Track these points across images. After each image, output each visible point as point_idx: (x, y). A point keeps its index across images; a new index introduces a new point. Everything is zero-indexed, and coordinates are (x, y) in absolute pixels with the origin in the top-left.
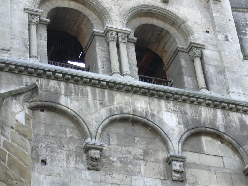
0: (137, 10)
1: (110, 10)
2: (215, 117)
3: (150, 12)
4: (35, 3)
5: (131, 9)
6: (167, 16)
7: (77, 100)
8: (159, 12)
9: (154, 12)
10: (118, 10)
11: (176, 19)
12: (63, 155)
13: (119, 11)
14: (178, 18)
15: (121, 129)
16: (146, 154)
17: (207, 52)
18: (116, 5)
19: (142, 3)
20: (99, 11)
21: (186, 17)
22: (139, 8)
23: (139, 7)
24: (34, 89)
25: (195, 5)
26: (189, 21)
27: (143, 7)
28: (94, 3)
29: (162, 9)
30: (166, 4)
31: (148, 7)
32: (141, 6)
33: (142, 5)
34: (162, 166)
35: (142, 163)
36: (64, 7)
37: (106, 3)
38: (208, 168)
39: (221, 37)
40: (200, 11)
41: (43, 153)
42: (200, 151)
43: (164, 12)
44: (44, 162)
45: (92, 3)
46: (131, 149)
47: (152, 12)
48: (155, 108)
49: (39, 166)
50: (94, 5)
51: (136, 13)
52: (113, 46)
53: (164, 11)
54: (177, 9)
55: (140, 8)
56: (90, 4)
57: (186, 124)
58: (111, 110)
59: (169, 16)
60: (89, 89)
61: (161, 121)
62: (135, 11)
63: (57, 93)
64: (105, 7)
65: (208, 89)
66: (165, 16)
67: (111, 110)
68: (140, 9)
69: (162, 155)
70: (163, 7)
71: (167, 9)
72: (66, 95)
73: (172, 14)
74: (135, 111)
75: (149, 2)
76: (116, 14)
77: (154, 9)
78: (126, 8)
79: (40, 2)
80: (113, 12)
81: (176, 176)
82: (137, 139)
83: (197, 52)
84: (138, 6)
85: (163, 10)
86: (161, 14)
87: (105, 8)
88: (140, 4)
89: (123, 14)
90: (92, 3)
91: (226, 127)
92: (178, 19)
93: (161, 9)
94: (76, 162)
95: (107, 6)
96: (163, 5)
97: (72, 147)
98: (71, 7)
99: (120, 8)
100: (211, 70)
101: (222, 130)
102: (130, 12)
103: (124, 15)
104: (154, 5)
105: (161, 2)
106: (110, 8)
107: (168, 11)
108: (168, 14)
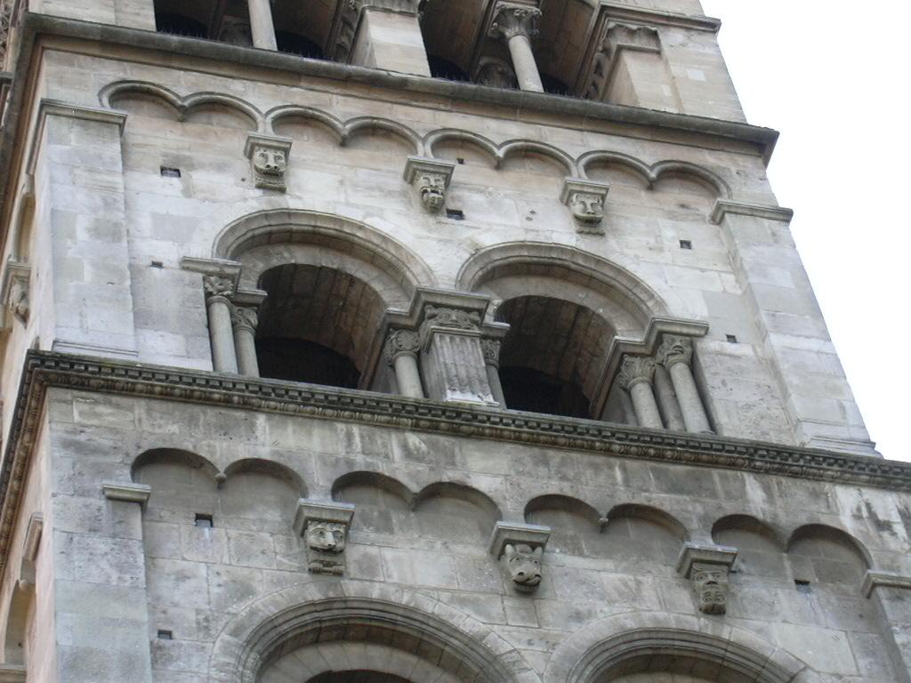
0: (613, 651)
1: (517, 664)
3: (662, 652)
4: (241, 669)
5: (591, 650)
6: (725, 664)
8: (696, 651)
9: (676, 652)
10: (545, 661)
11: (759, 668)
13: (547, 661)
14: (767, 665)
18: (536, 641)
19: (631, 624)
20: (476, 670)
21: (798, 659)
22: (621, 644)
23: (621, 641)
25: (824, 612)
26: (810, 672)
27: (637, 636)
28: (456, 642)
29: (705, 636)
30: (716, 618)
31: (654, 635)
32: (627, 636)
33: (633, 632)
36: (349, 669)
37: (500, 640)
40: (846, 632)
43: (712, 649)
45: (446, 645)
47: (670, 652)
50: (456, 649)
51: (612, 663)
53: (715, 643)
54: (759, 631)
55: (625, 643)
56: (442, 646)
59: (736, 663)
62: (607, 654)
64: (498, 653)
66: (720, 662)
68: (624, 647)
70: (709, 632)
71: (725, 636)
73: (742, 653)
75: (656, 619)
76: (541, 676)
77: (677, 643)
78: (573, 647)
79: (260, 663)
80: (528, 666)
84: (618, 637)
85: (708, 641)
86: (705, 657)
87: (495, 658)
88: (622, 627)
89: (565, 671)
90: (446, 645)
92: (768, 670)
93: (701, 640)
95: (502, 651)
96: (707, 622)
98: (371, 667)
99: (550, 651)
102: (590, 663)
103: (569, 674)
104: (674, 626)
105: (700, 613)
106: (514, 654)
107: (729, 643)
108: (728, 655)
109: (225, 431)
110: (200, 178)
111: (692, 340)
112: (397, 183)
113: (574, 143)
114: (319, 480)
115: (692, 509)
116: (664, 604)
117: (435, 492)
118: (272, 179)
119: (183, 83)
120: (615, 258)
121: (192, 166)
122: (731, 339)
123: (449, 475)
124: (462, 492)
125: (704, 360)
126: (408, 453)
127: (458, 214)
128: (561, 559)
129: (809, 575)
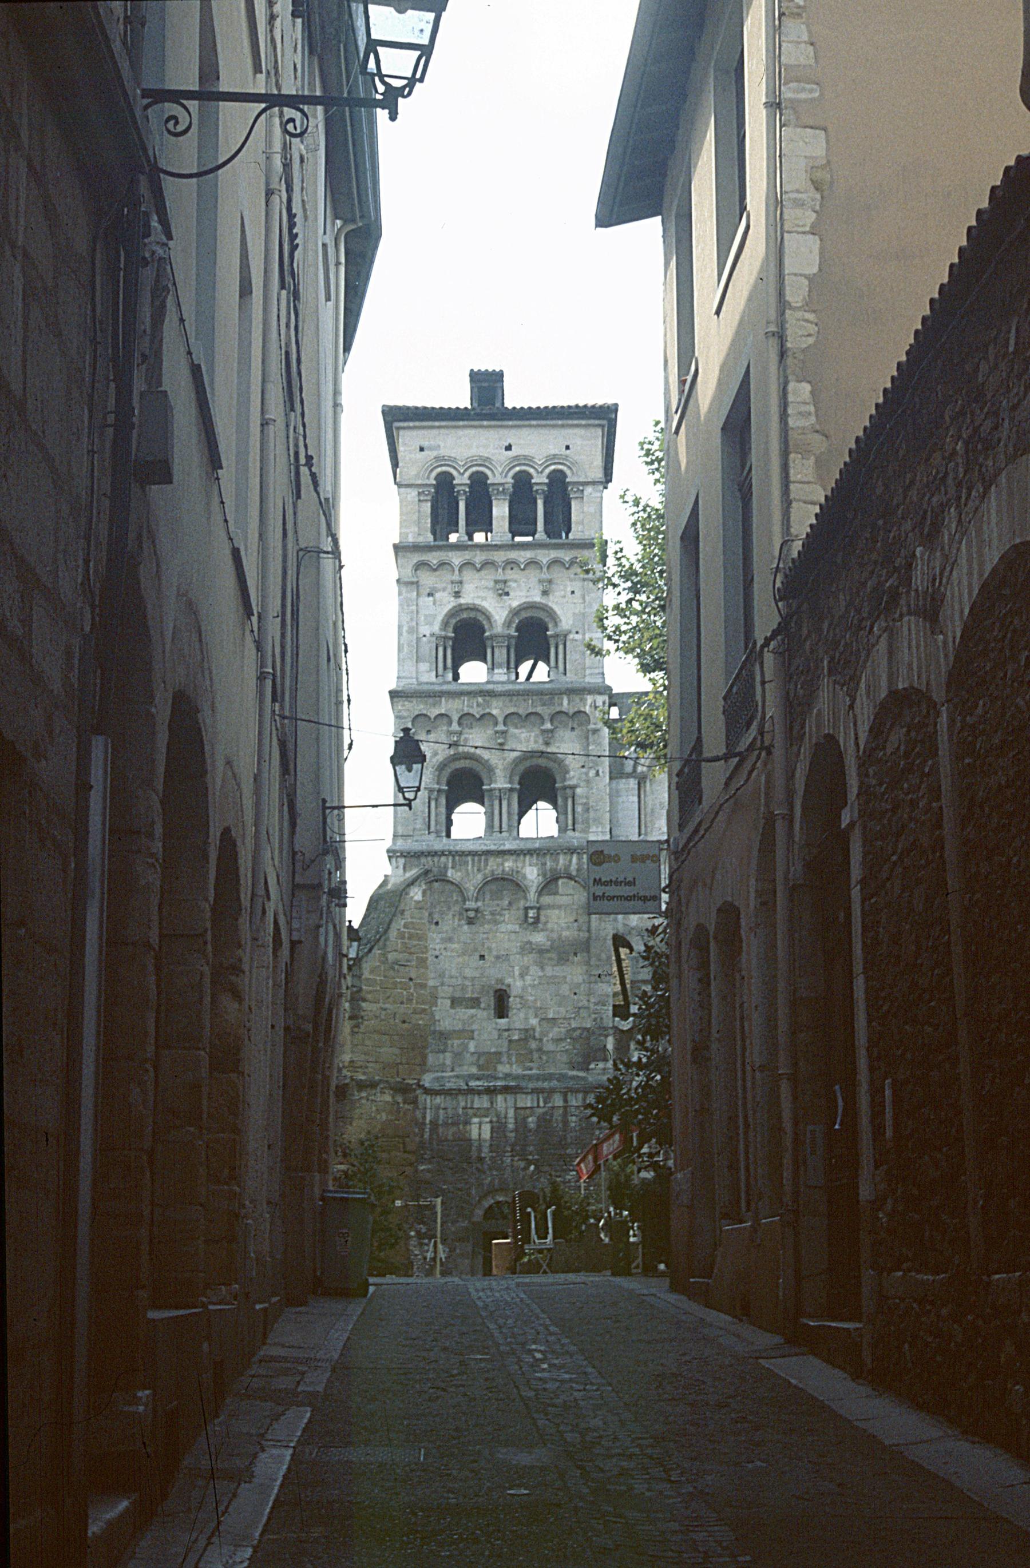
2: (570, 861)
7: (460, 870)
12: (450, 916)
15: (493, 887)
16: (510, 904)
17: (578, 791)
24: (427, 872)
34: (522, 912)
35: (506, 912)
38: (559, 907)
39: (592, 773)
41: (436, 917)
42: (556, 893)
44: (437, 923)
46: (499, 902)
48: (520, 865)
49: (433, 927)
52: (496, 803)
57: (544, 875)
58: (485, 874)
60: (469, 858)
61: (524, 877)
63: (446, 868)
65: (574, 830)
67: (485, 874)
69: (522, 904)
72: (453, 868)
74: (503, 871)
81: (531, 920)
82: (505, 892)
83: (569, 792)
91: (578, 870)
94: (459, 920)
97: (457, 908)
100: (579, 809)
101: (574, 873)
109: (434, 705)
110: (438, 595)
111: (566, 636)
112: (492, 584)
113: (545, 556)
114: (455, 718)
115: (545, 711)
116: (536, 742)
117: (483, 716)
118: (457, 594)
119: (434, 557)
120: (550, 604)
121: (437, 590)
122: (577, 633)
123: (488, 710)
124: (489, 714)
125: (568, 643)
126: (478, 705)
127: (507, 594)
128: (513, 730)
129: (575, 726)
